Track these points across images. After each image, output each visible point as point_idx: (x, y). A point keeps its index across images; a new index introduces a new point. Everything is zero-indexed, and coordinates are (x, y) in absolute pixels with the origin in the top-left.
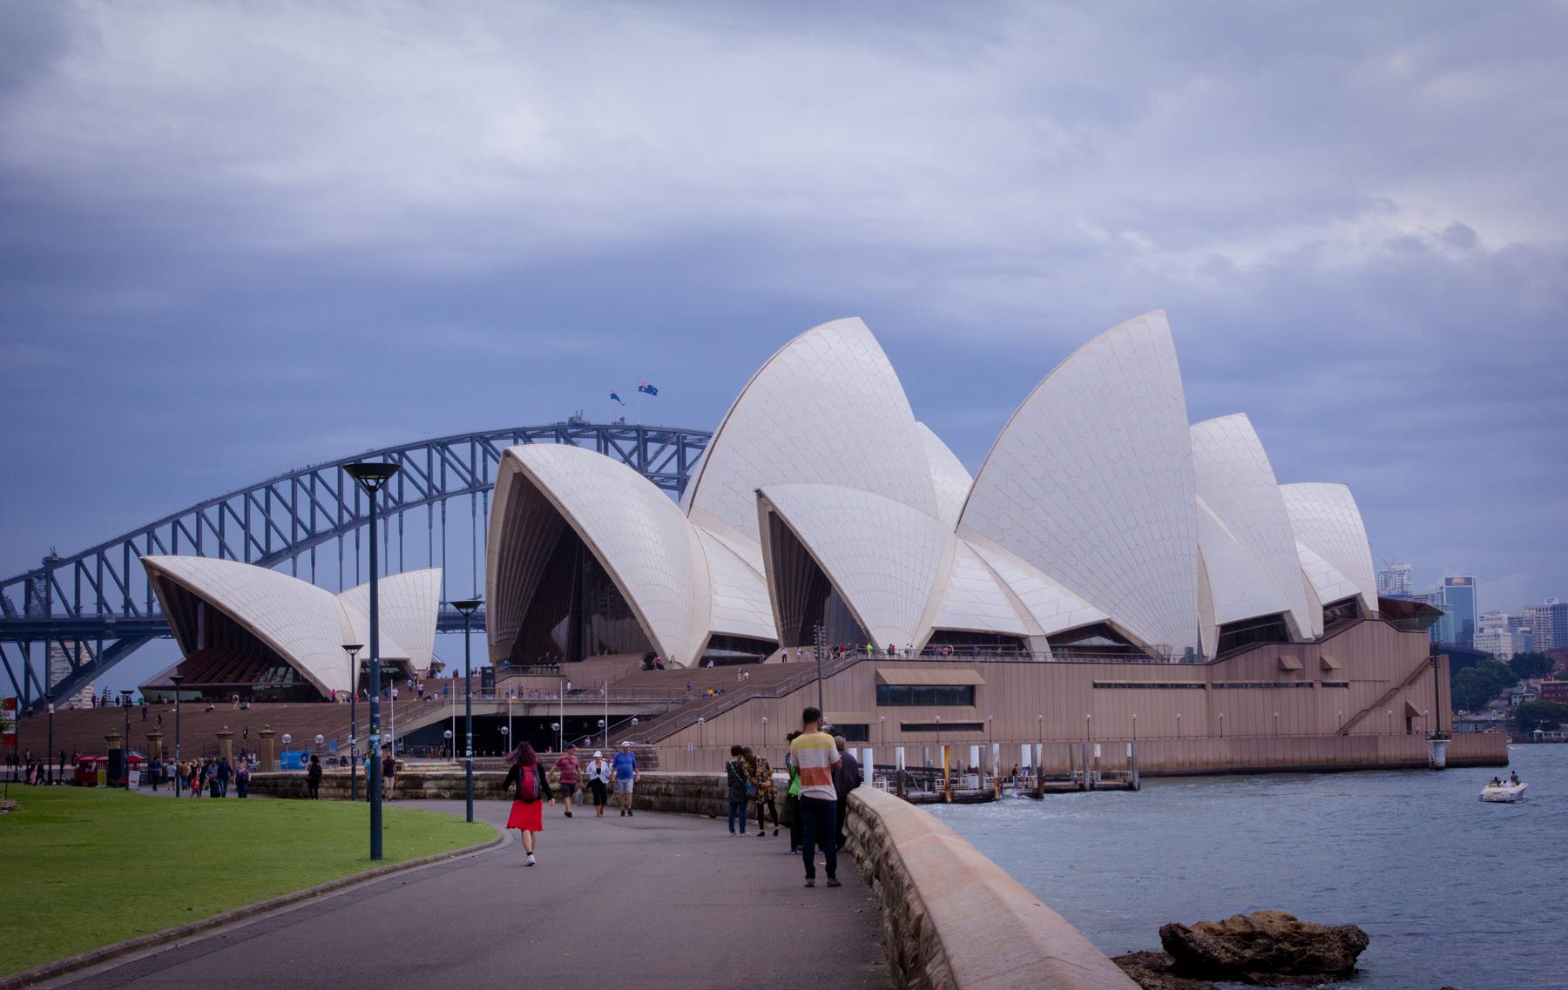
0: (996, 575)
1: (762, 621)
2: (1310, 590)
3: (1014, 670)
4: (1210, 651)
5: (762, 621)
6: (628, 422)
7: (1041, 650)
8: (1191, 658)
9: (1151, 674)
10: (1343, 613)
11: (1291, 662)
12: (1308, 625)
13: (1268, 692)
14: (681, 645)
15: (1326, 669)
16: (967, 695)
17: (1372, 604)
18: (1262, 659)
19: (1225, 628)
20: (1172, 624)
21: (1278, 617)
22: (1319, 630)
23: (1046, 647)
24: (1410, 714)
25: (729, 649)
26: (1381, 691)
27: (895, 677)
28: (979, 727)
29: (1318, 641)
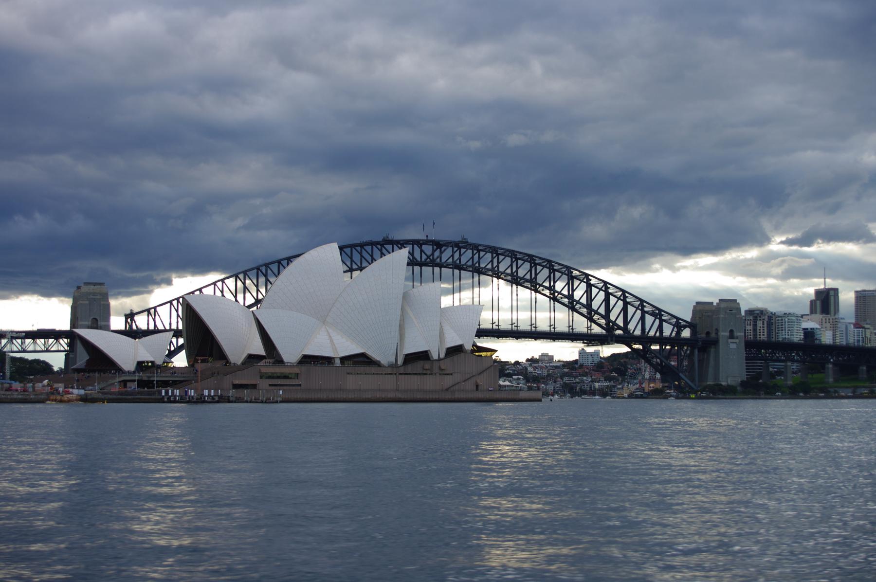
0: (330, 337)
1: (258, 348)
3: (317, 370)
4: (400, 361)
5: (258, 348)
6: (430, 238)
8: (394, 366)
11: (427, 366)
13: (419, 377)
14: (236, 356)
15: (441, 369)
18: (418, 366)
19: (407, 355)
22: (442, 356)
24: (477, 386)
25: (252, 358)
26: (468, 376)
28: (300, 385)
29: (440, 360)
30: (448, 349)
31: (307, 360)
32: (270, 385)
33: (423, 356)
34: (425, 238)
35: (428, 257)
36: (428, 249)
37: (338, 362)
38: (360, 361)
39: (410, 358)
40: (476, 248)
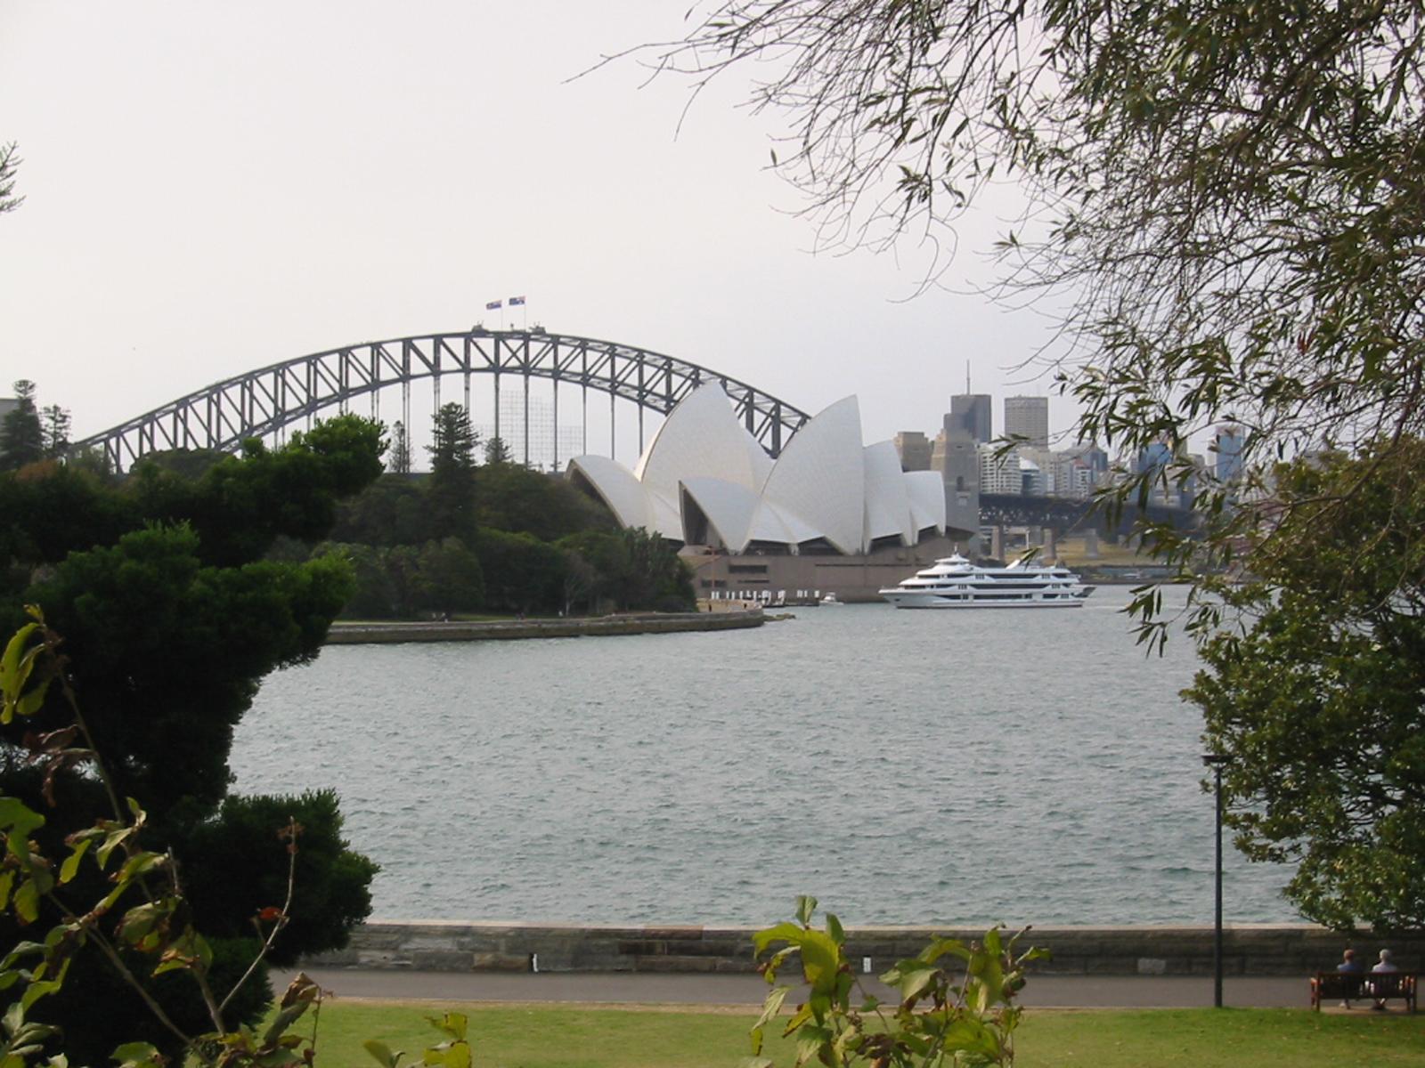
2: (913, 524)
3: (783, 560)
4: (866, 550)
7: (795, 549)
8: (860, 554)
9: (841, 560)
10: (928, 534)
11: (902, 555)
12: (911, 539)
15: (917, 559)
16: (763, 569)
17: (942, 529)
18: (888, 555)
19: (875, 540)
20: (849, 540)
21: (897, 536)
22: (916, 541)
23: (797, 549)
27: (736, 562)
29: (914, 546)
30: (921, 531)
31: (756, 546)
32: (740, 582)
33: (894, 541)
34: (508, 329)
35: (514, 354)
36: (515, 344)
37: (795, 549)
38: (819, 548)
39: (881, 544)
40: (556, 341)
